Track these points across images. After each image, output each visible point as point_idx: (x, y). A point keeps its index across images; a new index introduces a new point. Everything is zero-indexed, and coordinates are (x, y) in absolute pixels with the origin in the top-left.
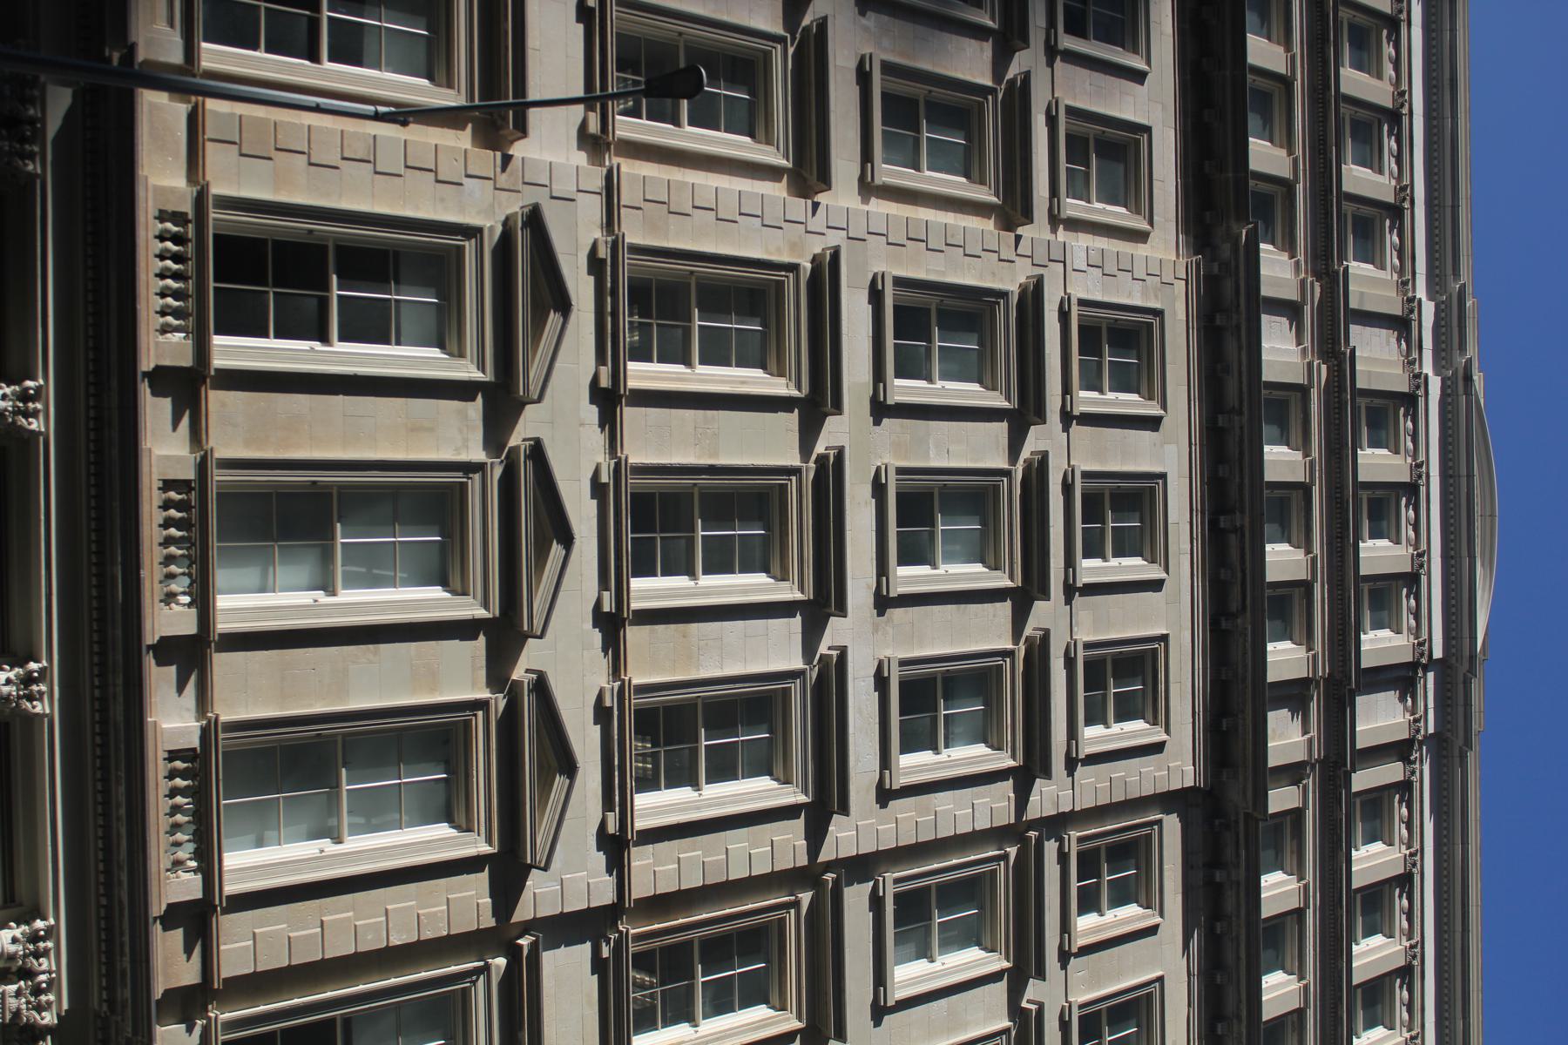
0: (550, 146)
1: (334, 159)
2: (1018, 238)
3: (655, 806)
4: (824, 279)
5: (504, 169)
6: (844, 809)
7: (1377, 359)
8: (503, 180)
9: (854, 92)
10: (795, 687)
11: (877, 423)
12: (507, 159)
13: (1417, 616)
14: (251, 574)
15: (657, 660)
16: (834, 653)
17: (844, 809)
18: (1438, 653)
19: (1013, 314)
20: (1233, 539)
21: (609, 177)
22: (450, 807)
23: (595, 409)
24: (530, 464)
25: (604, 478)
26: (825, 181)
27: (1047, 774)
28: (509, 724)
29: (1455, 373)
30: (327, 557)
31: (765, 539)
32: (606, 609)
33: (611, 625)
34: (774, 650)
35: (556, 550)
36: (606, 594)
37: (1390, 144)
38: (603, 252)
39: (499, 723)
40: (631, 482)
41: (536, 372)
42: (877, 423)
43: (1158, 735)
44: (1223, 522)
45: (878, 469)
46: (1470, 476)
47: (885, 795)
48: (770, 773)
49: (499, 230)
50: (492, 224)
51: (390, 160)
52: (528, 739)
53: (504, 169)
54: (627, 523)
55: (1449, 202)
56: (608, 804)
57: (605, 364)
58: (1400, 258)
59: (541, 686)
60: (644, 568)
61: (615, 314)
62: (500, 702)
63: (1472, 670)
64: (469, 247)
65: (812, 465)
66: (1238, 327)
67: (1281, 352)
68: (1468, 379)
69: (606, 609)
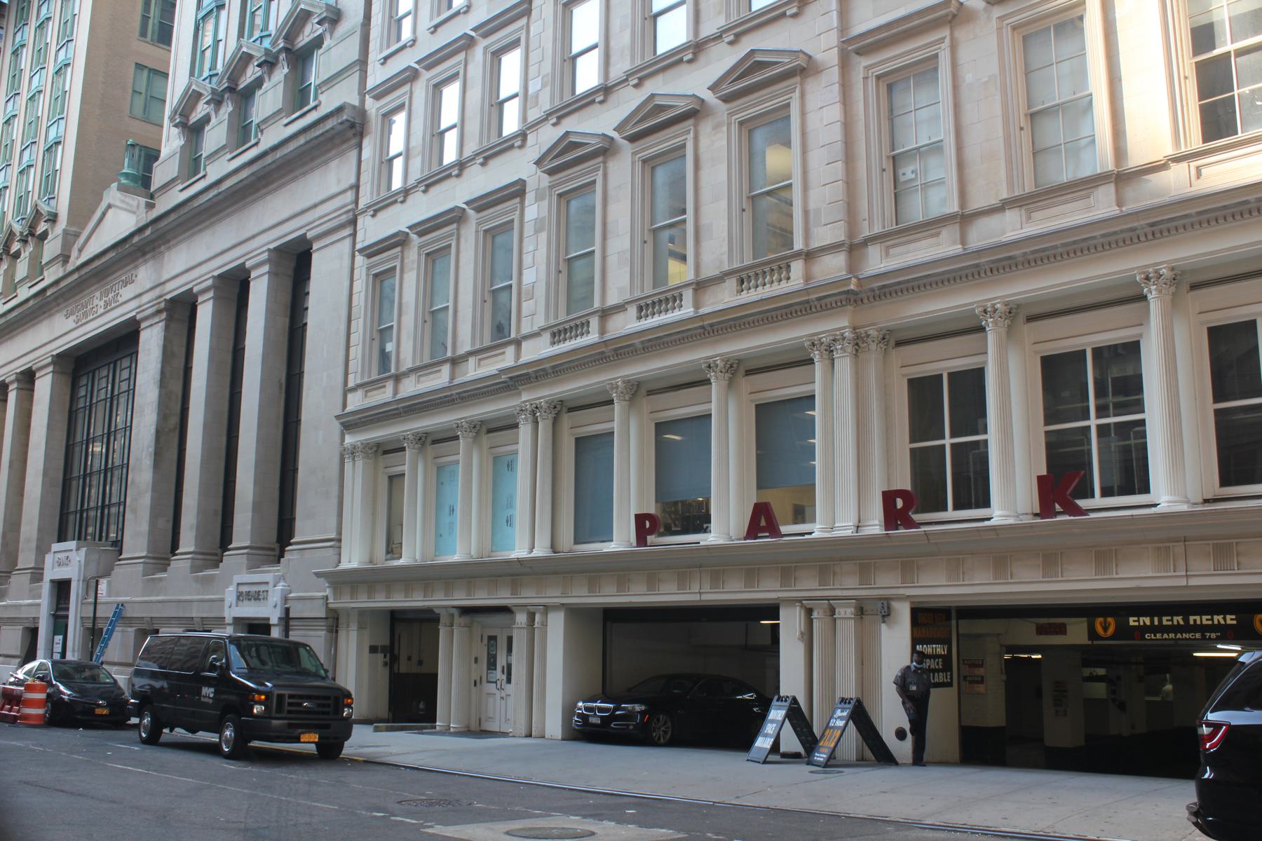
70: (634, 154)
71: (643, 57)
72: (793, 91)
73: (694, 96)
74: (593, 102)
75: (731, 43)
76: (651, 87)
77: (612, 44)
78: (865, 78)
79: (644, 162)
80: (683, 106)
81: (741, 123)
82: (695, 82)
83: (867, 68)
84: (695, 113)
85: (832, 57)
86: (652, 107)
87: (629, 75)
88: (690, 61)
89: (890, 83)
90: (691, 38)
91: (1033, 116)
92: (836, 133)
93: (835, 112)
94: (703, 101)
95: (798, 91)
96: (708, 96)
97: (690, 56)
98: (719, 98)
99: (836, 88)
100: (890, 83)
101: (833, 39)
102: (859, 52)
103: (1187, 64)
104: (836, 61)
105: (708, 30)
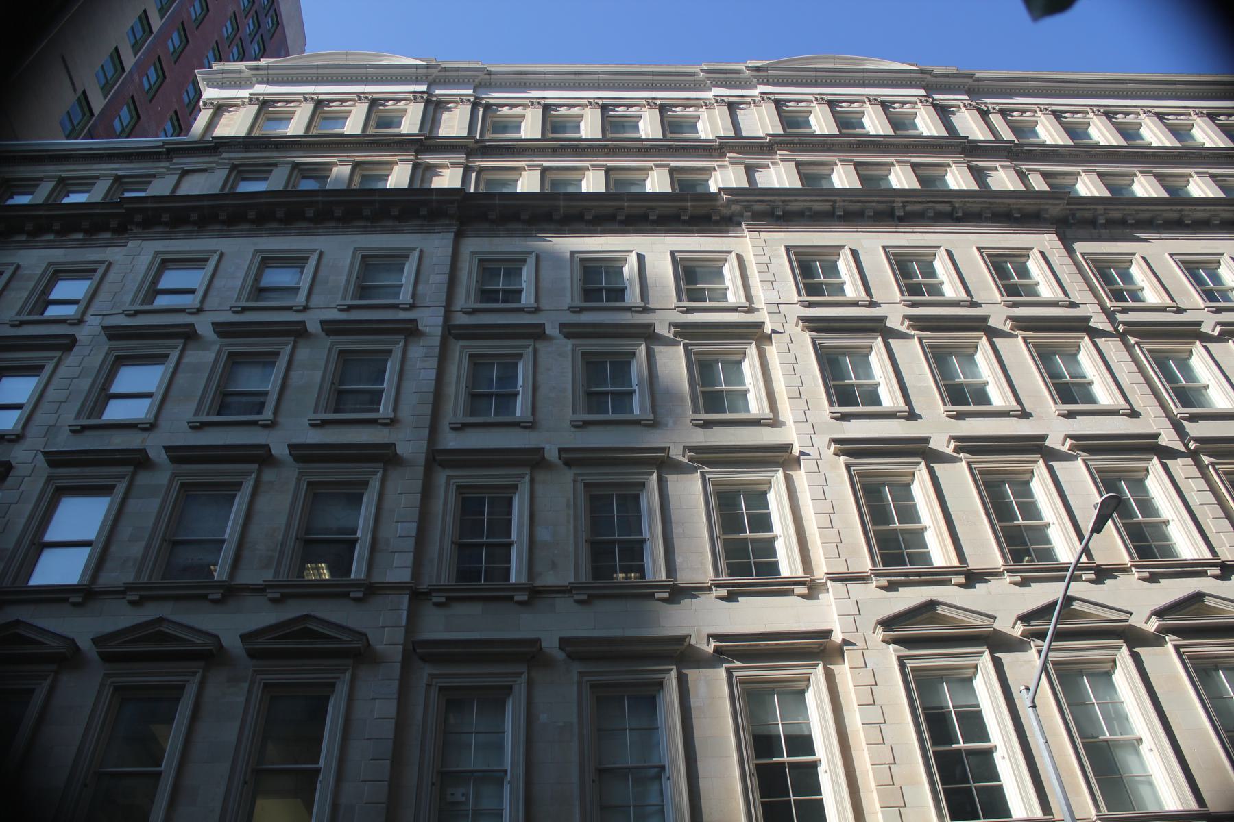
0: (828, 613)
1: (886, 748)
2: (773, 331)
3: (940, 554)
4: (851, 448)
5: (854, 644)
6: (926, 440)
7: (760, 122)
8: (861, 644)
9: (718, 431)
10: (1093, 465)
11: (920, 417)
12: (846, 642)
13: (904, 103)
14: (1144, 791)
15: (986, 550)
16: (833, 446)
17: (926, 440)
18: (922, 92)
19: (823, 335)
20: (909, 208)
21: (834, 580)
22: (1104, 676)
23: (977, 585)
24: (1033, 623)
25: (1018, 579)
26: (787, 448)
27: (985, 319)
28: (1183, 632)
29: (754, 76)
30: (1117, 744)
31: (891, 485)
32: (1093, 576)
33: (972, 578)
34: (959, 478)
35: (1076, 606)
36: (1084, 577)
37: (621, 111)
38: (884, 582)
39: (1184, 638)
40: (724, 578)
41: (978, 621)
42: (920, 417)
43: (846, 253)
44: (899, 213)
45: (948, 416)
46: (816, 70)
47: (912, 416)
48: (908, 485)
49: (891, 646)
50: (892, 651)
51: (874, 714)
52: (1060, 624)
53: (854, 644)
54: (746, 580)
55: (650, 78)
56: (1203, 574)
57: (653, 595)
58: (689, 106)
59: (1160, 613)
60: (773, 568)
61: (919, 574)
62: (1170, 639)
63: (930, 72)
64: (910, 664)
65: (962, 455)
66: (783, 201)
67: (779, 175)
68: (758, 69)
69: (1093, 576)
70: (106, 676)
71: (150, 577)
72: (194, 674)
73: (73, 640)
74: (66, 600)
75: (273, 601)
76: (150, 612)
77: (113, 548)
78: (429, 686)
79: (117, 689)
80: (198, 643)
81: (266, 686)
82: (229, 626)
83: (432, 676)
84: (210, 655)
85: (397, 653)
86: (154, 631)
87: (128, 588)
88: (215, 602)
89: (455, 701)
90: (86, 582)
91: (602, 771)
92: (388, 730)
93: (389, 708)
94: (78, 649)
95: (49, 681)
96: (85, 644)
97: (218, 596)
98: (100, 654)
99: (396, 684)
100: (455, 701)
101: (400, 635)
102: (425, 659)
103: (751, 763)
104: (399, 658)
105: (113, 577)
